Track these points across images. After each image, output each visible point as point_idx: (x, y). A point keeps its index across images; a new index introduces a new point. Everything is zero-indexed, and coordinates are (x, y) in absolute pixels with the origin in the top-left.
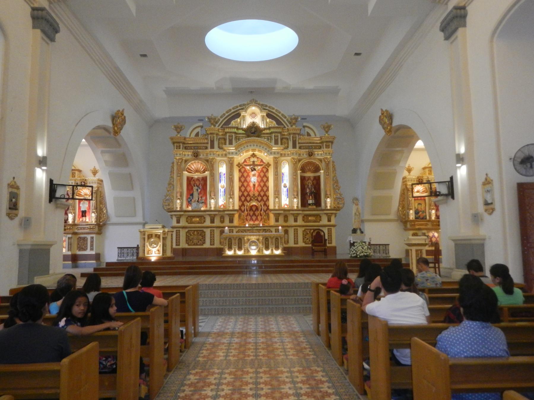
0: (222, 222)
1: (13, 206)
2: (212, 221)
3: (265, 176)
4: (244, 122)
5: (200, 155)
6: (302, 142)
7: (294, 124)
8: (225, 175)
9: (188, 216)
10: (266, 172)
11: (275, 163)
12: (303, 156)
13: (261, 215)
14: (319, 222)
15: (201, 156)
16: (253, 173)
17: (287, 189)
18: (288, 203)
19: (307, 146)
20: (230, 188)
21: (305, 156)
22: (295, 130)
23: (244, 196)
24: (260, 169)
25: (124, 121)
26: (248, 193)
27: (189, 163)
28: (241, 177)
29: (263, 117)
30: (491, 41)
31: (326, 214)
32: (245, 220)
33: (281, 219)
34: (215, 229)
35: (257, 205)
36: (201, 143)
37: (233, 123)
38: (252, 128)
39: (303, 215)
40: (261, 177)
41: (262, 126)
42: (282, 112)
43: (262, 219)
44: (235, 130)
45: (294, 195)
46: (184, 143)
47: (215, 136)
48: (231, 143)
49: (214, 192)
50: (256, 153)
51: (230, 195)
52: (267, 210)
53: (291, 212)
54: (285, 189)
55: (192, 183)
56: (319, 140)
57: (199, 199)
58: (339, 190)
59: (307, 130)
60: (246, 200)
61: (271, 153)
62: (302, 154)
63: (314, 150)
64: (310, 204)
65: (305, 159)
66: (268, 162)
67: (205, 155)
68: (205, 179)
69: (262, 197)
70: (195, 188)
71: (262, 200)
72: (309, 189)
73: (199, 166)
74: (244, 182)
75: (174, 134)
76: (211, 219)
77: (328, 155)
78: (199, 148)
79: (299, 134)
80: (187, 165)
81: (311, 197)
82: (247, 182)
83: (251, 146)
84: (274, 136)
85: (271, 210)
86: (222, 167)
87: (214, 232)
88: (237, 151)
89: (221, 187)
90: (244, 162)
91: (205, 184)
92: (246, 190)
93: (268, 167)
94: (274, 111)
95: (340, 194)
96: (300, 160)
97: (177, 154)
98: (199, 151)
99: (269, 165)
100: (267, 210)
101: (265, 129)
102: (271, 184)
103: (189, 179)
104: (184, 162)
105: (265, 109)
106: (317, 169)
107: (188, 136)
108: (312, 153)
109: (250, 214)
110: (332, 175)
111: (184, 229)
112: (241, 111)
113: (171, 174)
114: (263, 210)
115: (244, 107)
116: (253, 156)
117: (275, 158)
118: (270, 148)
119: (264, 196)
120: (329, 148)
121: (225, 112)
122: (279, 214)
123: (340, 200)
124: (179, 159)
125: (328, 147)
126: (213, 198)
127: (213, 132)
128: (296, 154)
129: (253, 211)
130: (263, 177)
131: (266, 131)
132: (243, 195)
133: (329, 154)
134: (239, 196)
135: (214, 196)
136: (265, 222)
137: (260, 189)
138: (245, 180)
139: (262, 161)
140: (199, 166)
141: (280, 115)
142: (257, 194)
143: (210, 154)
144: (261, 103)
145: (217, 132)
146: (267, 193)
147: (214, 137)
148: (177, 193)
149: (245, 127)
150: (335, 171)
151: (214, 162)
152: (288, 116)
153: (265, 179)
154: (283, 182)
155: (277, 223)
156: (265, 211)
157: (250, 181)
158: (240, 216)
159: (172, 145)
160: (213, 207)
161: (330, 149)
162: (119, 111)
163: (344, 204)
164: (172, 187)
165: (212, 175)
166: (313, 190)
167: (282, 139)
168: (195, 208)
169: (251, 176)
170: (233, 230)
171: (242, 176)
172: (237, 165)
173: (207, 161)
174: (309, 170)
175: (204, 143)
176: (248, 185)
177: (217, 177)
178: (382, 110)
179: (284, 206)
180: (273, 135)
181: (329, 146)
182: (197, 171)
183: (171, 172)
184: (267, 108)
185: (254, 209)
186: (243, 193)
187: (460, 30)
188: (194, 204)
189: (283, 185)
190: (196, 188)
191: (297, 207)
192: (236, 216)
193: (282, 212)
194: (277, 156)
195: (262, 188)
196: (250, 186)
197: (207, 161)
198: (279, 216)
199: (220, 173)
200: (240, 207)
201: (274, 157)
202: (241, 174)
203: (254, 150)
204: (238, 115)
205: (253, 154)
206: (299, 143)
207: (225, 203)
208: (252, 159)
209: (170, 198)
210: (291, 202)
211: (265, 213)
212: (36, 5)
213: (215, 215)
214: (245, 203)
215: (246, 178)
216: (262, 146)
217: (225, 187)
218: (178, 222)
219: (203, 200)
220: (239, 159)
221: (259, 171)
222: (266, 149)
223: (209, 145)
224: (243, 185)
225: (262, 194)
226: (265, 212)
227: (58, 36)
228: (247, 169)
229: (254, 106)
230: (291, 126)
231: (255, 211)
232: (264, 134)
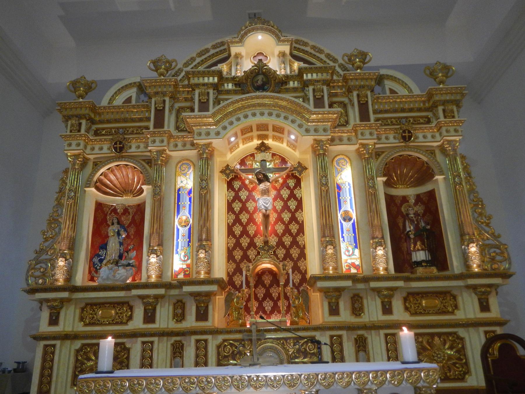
0: (180, 317)
2: (149, 318)
3: (292, 196)
4: (238, 67)
5: (130, 147)
7: (359, 67)
8: (192, 195)
9: (87, 304)
10: (295, 187)
11: (319, 155)
12: (387, 142)
13: (287, 298)
14: (452, 313)
15: (133, 149)
16: (262, 186)
17: (353, 224)
19: (395, 118)
20: (202, 222)
21: (392, 140)
22: (362, 79)
23: (241, 248)
24: (281, 180)
26: (252, 239)
27: (101, 168)
28: (233, 201)
29: (283, 55)
31: (474, 288)
32: (242, 311)
33: (344, 306)
34: (155, 339)
35: (275, 269)
38: (258, 74)
39: (405, 294)
40: (282, 199)
42: (327, 51)
43: (289, 307)
45: (373, 238)
47: (167, 99)
50: (270, 142)
51: (200, 240)
52: (300, 284)
53: (373, 284)
54: (347, 226)
56: (424, 102)
57: (121, 257)
58: (488, 225)
60: (245, 257)
61: (307, 131)
62: (383, 137)
63: (414, 126)
64: (419, 264)
66: (299, 163)
67: (142, 145)
68: (140, 209)
69: (288, 250)
70: (112, 230)
71: (288, 256)
72: (412, 221)
73: (130, 176)
74: (241, 212)
76: (145, 310)
77: (453, 133)
80: (95, 174)
81: (419, 243)
82: (248, 212)
83: (254, 115)
84: (314, 90)
85: (316, 279)
86: (185, 175)
87: (151, 350)
88: (219, 129)
89: (180, 223)
92: (244, 232)
93: (300, 173)
94: (308, 49)
95: (493, 234)
96: (378, 154)
97: (70, 145)
98: (126, 136)
99: (301, 168)
100: (300, 284)
101: (287, 79)
103: (99, 206)
104: (90, 165)
108: (409, 132)
109: (256, 295)
111: (68, 342)
113: (57, 198)
114: (291, 284)
116: (263, 148)
119: (291, 246)
120: (453, 117)
121: (194, 55)
122: (339, 290)
123: (498, 251)
124: (76, 156)
126: (153, 252)
128: (371, 134)
129: (264, 286)
130: (289, 199)
131: (291, 84)
132: (238, 244)
133: (456, 131)
134: (228, 248)
135: (159, 245)
136: (297, 316)
137: (280, 228)
138: (244, 209)
139: (284, 161)
140: (130, 176)
142: (273, 241)
143: (154, 141)
145: (171, 89)
146: (299, 239)
147: (164, 101)
150: (470, 177)
151: (162, 160)
153: (292, 204)
154: (340, 208)
155: (334, 319)
156: (297, 287)
157: (256, 209)
158: (228, 301)
160: (154, 276)
163: (509, 260)
164: (57, 230)
166: (422, 224)
168: (108, 278)
169: (256, 195)
170: (206, 341)
171: (237, 198)
174: (403, 181)
175: (140, 120)
176: (251, 220)
177: (172, 199)
179: (349, 269)
180: (311, 88)
181: (452, 111)
183: (60, 191)
185: (267, 279)
186: (238, 239)
188: (104, 271)
190: (116, 227)
191: (386, 269)
192: (219, 300)
193: (348, 283)
194: (324, 138)
195: (287, 226)
196: (255, 223)
197: (149, 162)
198: (338, 298)
199: (179, 190)
200: (230, 276)
201: (315, 140)
202: (233, 194)
205: (263, 144)
207: (188, 266)
208: (259, 157)
209: (48, 257)
211: (298, 291)
213: (157, 298)
214: (243, 266)
215: (244, 203)
216: (283, 115)
217: (191, 222)
218: (54, 321)
219: (131, 259)
221: (277, 185)
222: (293, 122)
223: (151, 124)
224: (238, 220)
225: (287, 240)
226: (297, 288)
228: (247, 182)
231: (271, 286)
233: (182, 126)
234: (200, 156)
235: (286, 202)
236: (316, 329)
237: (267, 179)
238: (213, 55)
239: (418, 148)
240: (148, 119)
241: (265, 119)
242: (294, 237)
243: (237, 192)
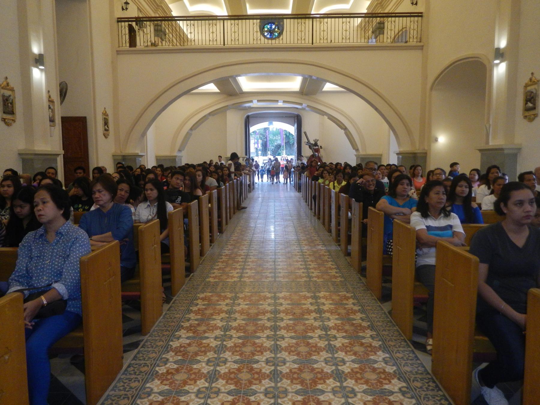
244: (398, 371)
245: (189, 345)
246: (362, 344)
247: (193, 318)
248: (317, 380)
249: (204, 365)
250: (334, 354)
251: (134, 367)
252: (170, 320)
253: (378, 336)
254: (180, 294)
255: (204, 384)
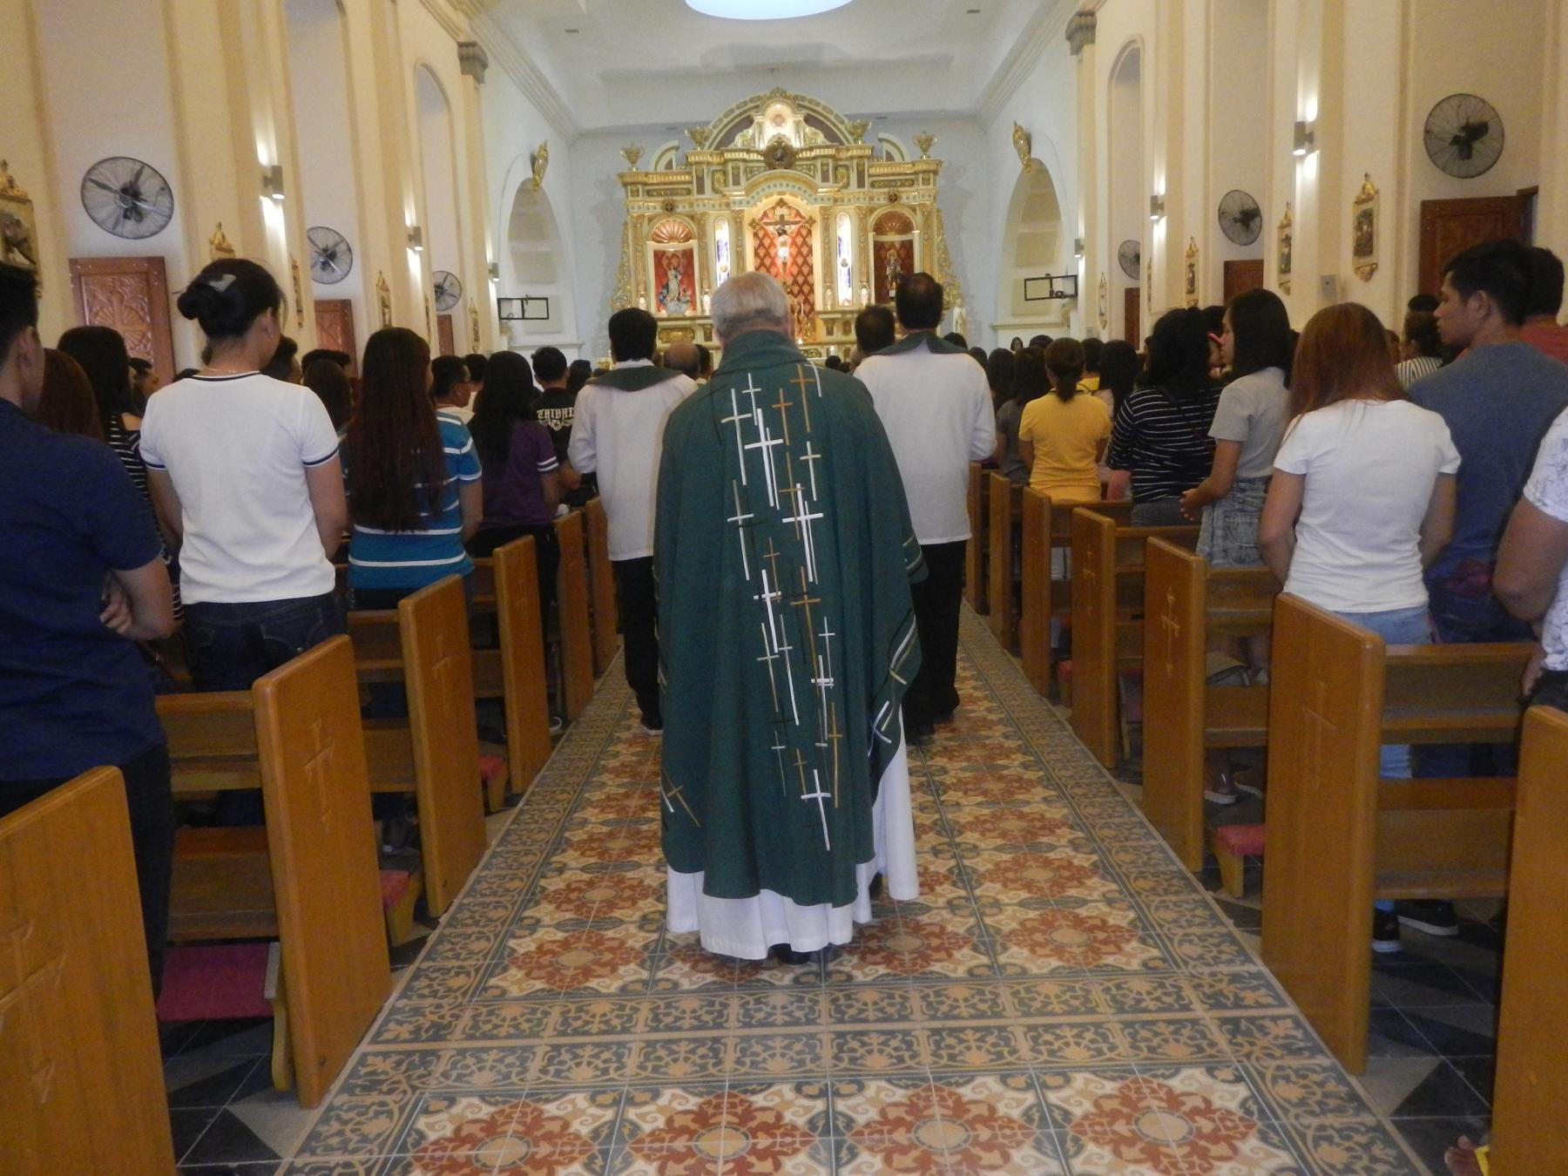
1: (477, 340)
3: (805, 243)
6: (878, 171)
7: (860, 136)
13: (799, 322)
15: (680, 209)
16: (782, 238)
18: (850, 298)
21: (883, 201)
25: (546, 160)
29: (797, 124)
30: (1109, 86)
36: (677, 183)
37: (738, 141)
41: (796, 143)
42: (836, 112)
44: (744, 155)
46: (645, 184)
47: (705, 167)
48: (736, 182)
49: (709, 279)
50: (787, 198)
54: (845, 270)
55: (665, 262)
59: (887, 147)
65: (883, 208)
68: (688, 254)
69: (801, 287)
70: (671, 273)
71: (801, 291)
75: (624, 166)
78: (673, 192)
79: (869, 157)
85: (820, 313)
90: (762, 219)
91: (690, 264)
94: (819, 109)
99: (812, 221)
101: (802, 150)
102: (817, 260)
105: (800, 106)
106: (906, 227)
107: (651, 169)
110: (937, 239)
112: (752, 113)
115: (759, 105)
117: (824, 210)
118: (814, 188)
122: (834, 320)
124: (639, 217)
125: (926, 182)
127: (701, 159)
137: (795, 270)
138: (767, 254)
139: (798, 214)
141: (832, 118)
142: (790, 280)
144: (791, 92)
146: (809, 278)
148: (638, 285)
149: (763, 145)
152: (849, 117)
153: (805, 250)
155: (830, 338)
156: (807, 315)
157: (776, 255)
159: (623, 190)
161: (931, 186)
162: (541, 147)
165: (703, 248)
166: (899, 268)
167: (836, 169)
171: (761, 245)
172: (750, 225)
173: (692, 218)
174: (892, 229)
176: (773, 264)
178: (1016, 124)
180: (818, 163)
182: (672, 238)
184: (806, 104)
187: (1086, 48)
188: (672, 305)
189: (839, 261)
193: (839, 316)
195: (800, 268)
203: (783, 193)
204: (749, 122)
205: (781, 200)
206: (870, 176)
208: (780, 211)
210: (856, 295)
212: (462, 39)
215: (767, 250)
220: (754, 211)
225: (800, 279)
227: (487, 73)
229: (777, 102)
230: (856, 141)
232: (801, 159)
233: (717, 185)
234: (735, 219)
235: (799, 248)
236: (819, 344)
237: (785, 232)
238: (741, 114)
239: (903, 205)
240: (691, 182)
241: (784, 189)
242: (806, 277)
243: (761, 241)
244: (1141, 921)
245: (591, 884)
246: (1047, 863)
247: (593, 819)
248: (929, 952)
249: (633, 929)
250: (972, 888)
251: (452, 943)
252: (533, 826)
253: (1089, 842)
254: (554, 762)
255: (636, 973)
